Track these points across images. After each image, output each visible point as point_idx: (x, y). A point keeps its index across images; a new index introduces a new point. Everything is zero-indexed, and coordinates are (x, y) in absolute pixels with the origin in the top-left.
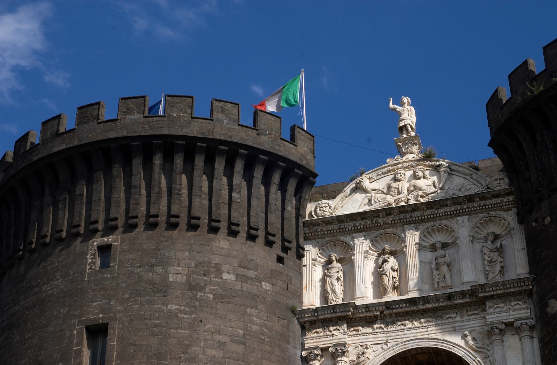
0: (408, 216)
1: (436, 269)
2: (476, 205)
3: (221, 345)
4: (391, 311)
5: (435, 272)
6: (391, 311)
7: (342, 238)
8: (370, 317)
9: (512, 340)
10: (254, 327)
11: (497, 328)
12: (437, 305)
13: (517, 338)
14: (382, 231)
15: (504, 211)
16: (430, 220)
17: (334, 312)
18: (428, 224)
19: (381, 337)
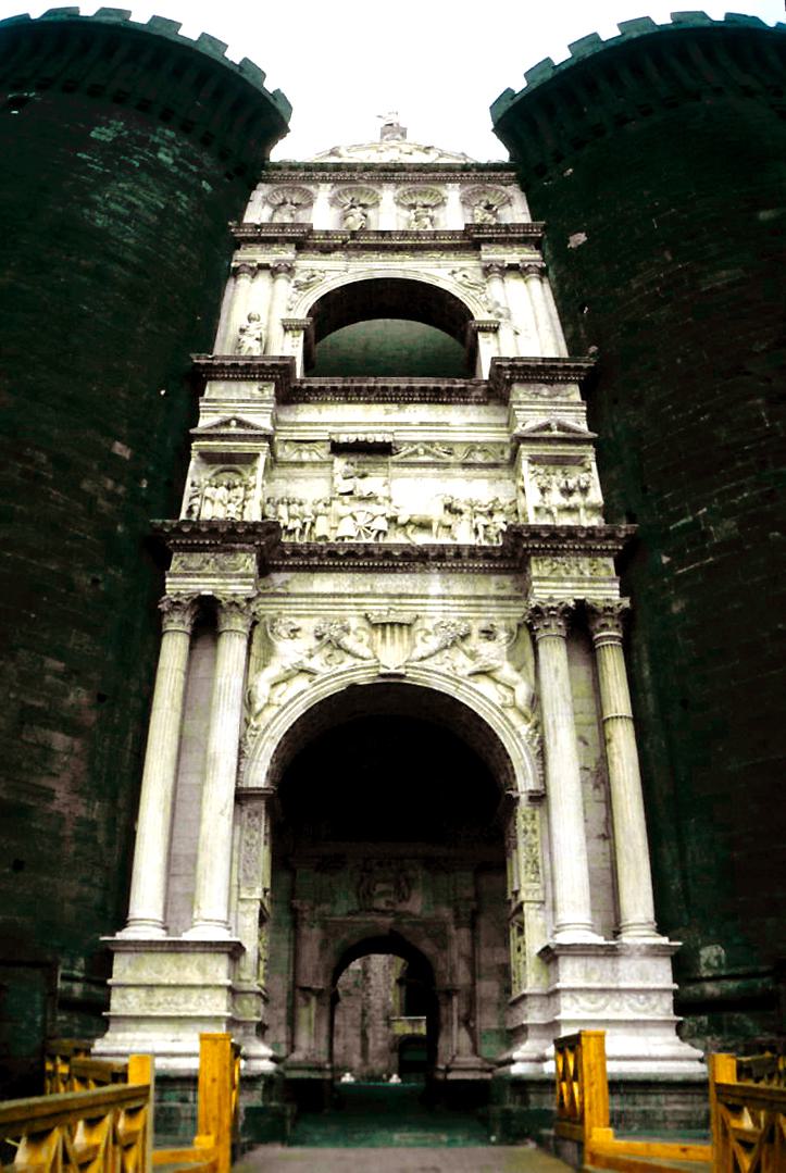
0: (389, 174)
1: (416, 221)
2: (471, 174)
3: (131, 206)
4: (356, 242)
5: (413, 223)
6: (356, 242)
7: (304, 186)
8: (328, 246)
9: (514, 284)
10: (179, 210)
11: (498, 266)
12: (418, 242)
13: (520, 282)
14: (355, 186)
15: (506, 185)
16: (413, 182)
17: (283, 232)
18: (410, 186)
19: (341, 265)
